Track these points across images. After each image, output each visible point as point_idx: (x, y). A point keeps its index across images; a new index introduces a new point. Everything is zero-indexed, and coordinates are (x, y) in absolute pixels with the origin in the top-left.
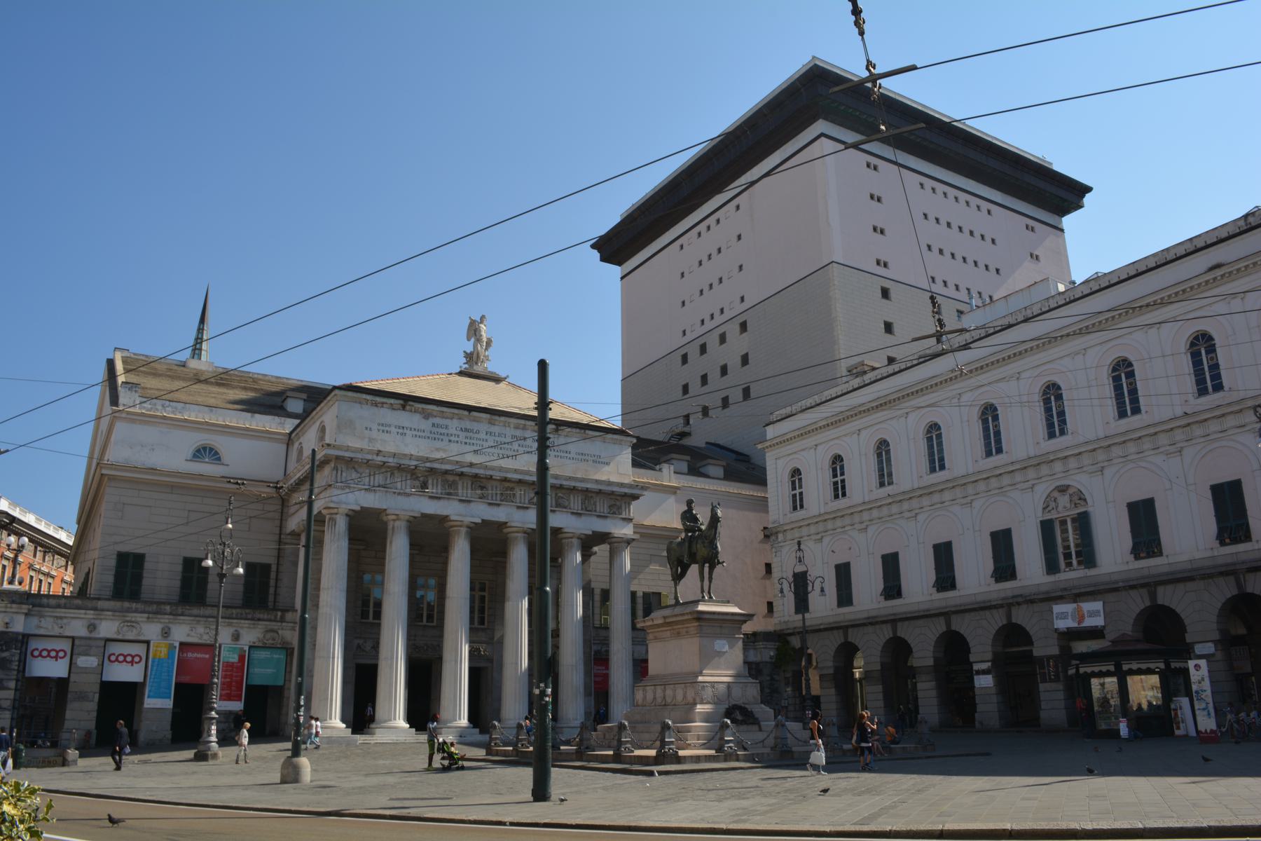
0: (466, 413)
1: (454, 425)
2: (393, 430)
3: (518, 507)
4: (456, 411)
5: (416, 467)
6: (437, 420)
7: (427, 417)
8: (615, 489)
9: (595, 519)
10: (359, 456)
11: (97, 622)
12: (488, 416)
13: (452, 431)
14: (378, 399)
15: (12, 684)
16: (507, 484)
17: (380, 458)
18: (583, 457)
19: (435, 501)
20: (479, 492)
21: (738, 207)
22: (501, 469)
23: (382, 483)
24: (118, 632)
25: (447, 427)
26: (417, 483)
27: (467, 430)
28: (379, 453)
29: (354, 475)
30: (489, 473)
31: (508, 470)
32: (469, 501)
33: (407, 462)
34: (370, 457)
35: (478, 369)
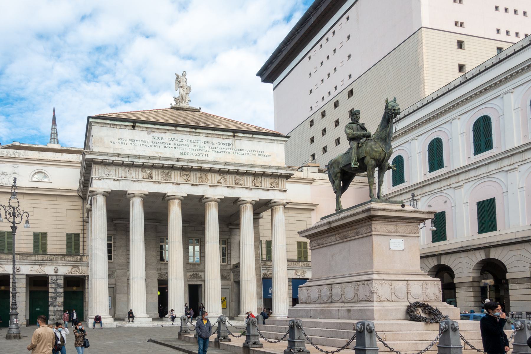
0: (173, 128)
2: (128, 142)
3: (211, 186)
5: (143, 163)
6: (156, 134)
9: (261, 191)
12: (188, 130)
13: (167, 141)
17: (120, 159)
19: (158, 185)
20: (185, 177)
21: (348, 18)
22: (197, 161)
23: (123, 176)
25: (162, 138)
27: (175, 140)
28: (119, 155)
29: (106, 172)
30: (191, 164)
31: (202, 162)
32: (179, 184)
33: (137, 160)
34: (113, 158)
35: (183, 105)
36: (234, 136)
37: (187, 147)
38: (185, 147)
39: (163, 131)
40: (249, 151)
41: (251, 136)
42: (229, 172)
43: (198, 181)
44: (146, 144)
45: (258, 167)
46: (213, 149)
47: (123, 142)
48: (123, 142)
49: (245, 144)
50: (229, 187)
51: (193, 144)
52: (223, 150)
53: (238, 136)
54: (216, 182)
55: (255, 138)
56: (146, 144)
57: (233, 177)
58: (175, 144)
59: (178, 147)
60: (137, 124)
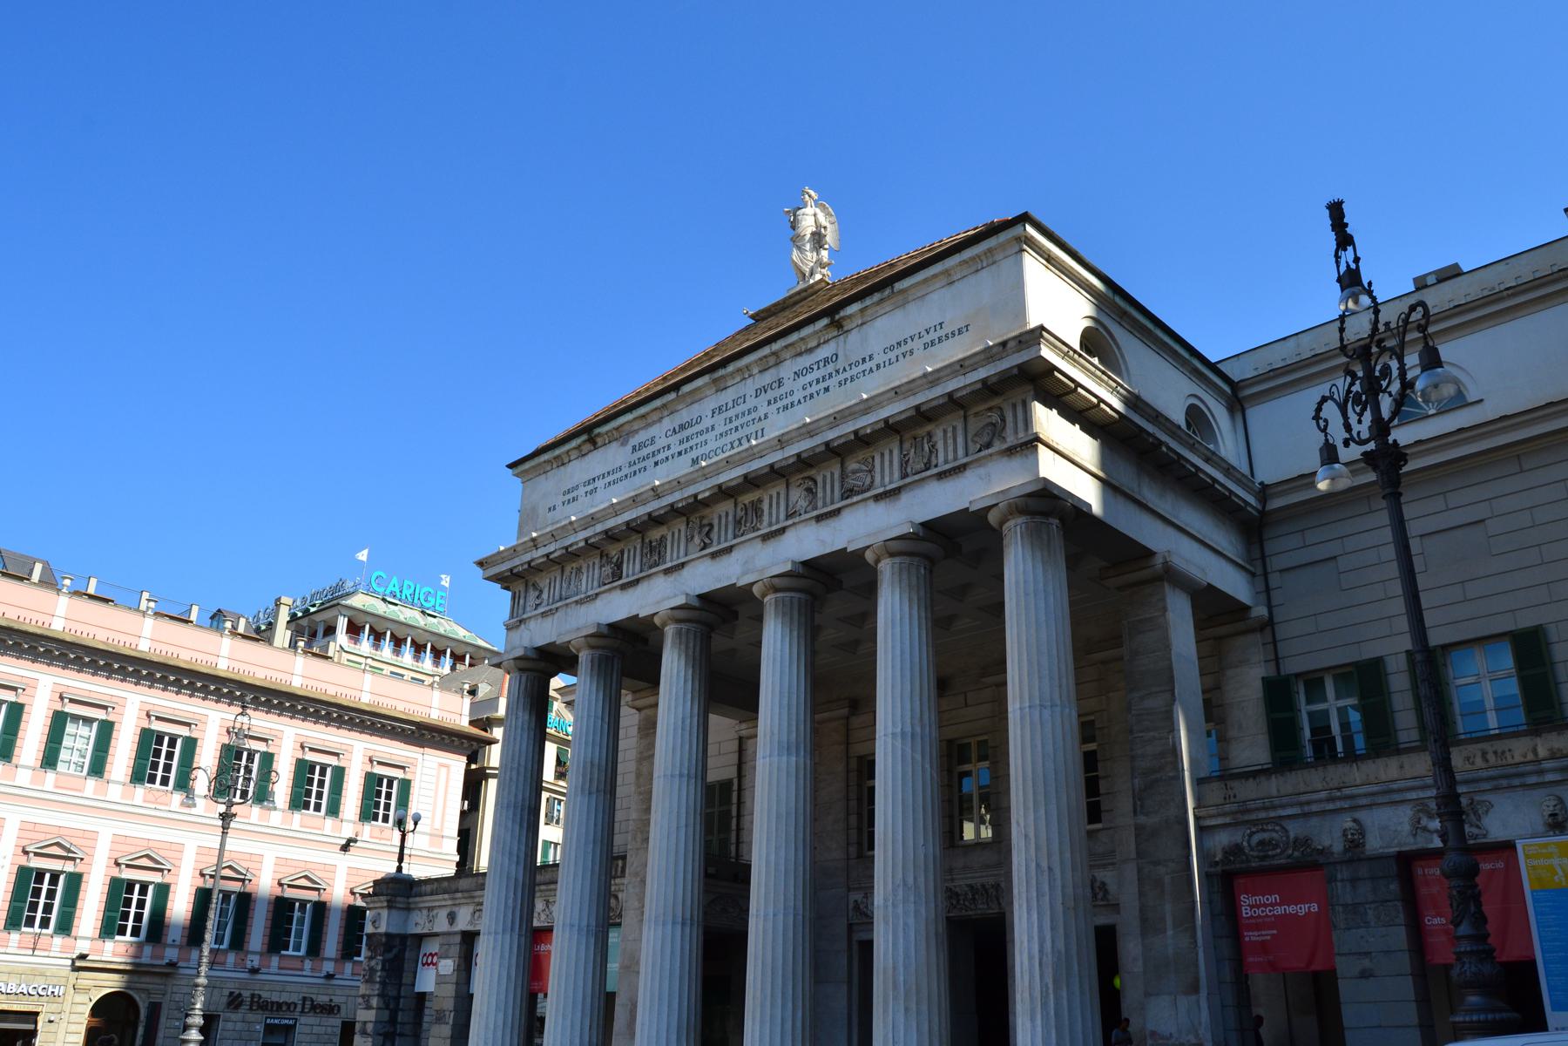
1: (660, 432)
3: (766, 538)
4: (658, 403)
5: (586, 540)
6: (642, 437)
7: (623, 444)
8: (951, 385)
10: (517, 562)
11: (455, 909)
12: (706, 379)
14: (557, 452)
15: (374, 1002)
16: (747, 499)
18: (900, 348)
24: (471, 923)
26: (608, 570)
27: (682, 427)
36: (838, 325)
37: (710, 436)
38: (701, 438)
39: (655, 416)
40: (892, 348)
41: (887, 292)
42: (804, 464)
43: (730, 535)
44: (619, 475)
45: (890, 401)
46: (780, 404)
47: (570, 496)
48: (570, 496)
49: (880, 330)
50: (819, 519)
51: (724, 415)
52: (809, 390)
53: (850, 317)
54: (782, 516)
55: (903, 291)
56: (619, 475)
57: (837, 476)
58: (681, 442)
59: (691, 443)
60: (597, 431)
